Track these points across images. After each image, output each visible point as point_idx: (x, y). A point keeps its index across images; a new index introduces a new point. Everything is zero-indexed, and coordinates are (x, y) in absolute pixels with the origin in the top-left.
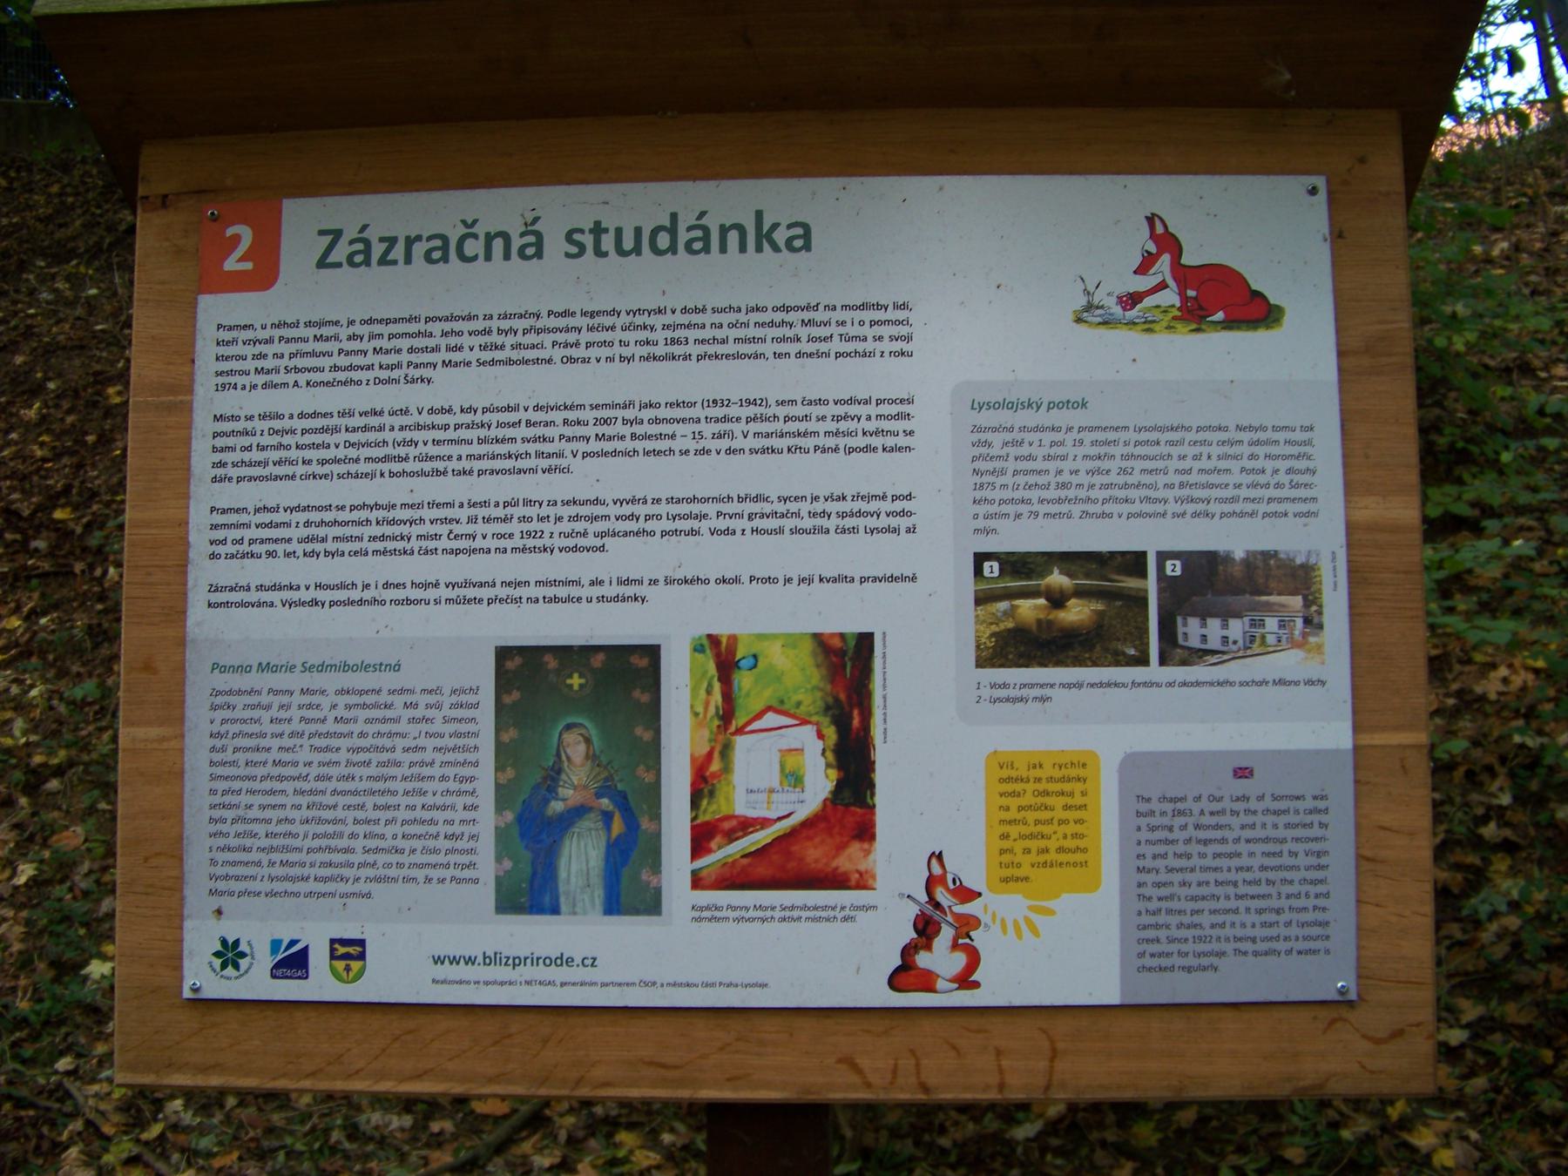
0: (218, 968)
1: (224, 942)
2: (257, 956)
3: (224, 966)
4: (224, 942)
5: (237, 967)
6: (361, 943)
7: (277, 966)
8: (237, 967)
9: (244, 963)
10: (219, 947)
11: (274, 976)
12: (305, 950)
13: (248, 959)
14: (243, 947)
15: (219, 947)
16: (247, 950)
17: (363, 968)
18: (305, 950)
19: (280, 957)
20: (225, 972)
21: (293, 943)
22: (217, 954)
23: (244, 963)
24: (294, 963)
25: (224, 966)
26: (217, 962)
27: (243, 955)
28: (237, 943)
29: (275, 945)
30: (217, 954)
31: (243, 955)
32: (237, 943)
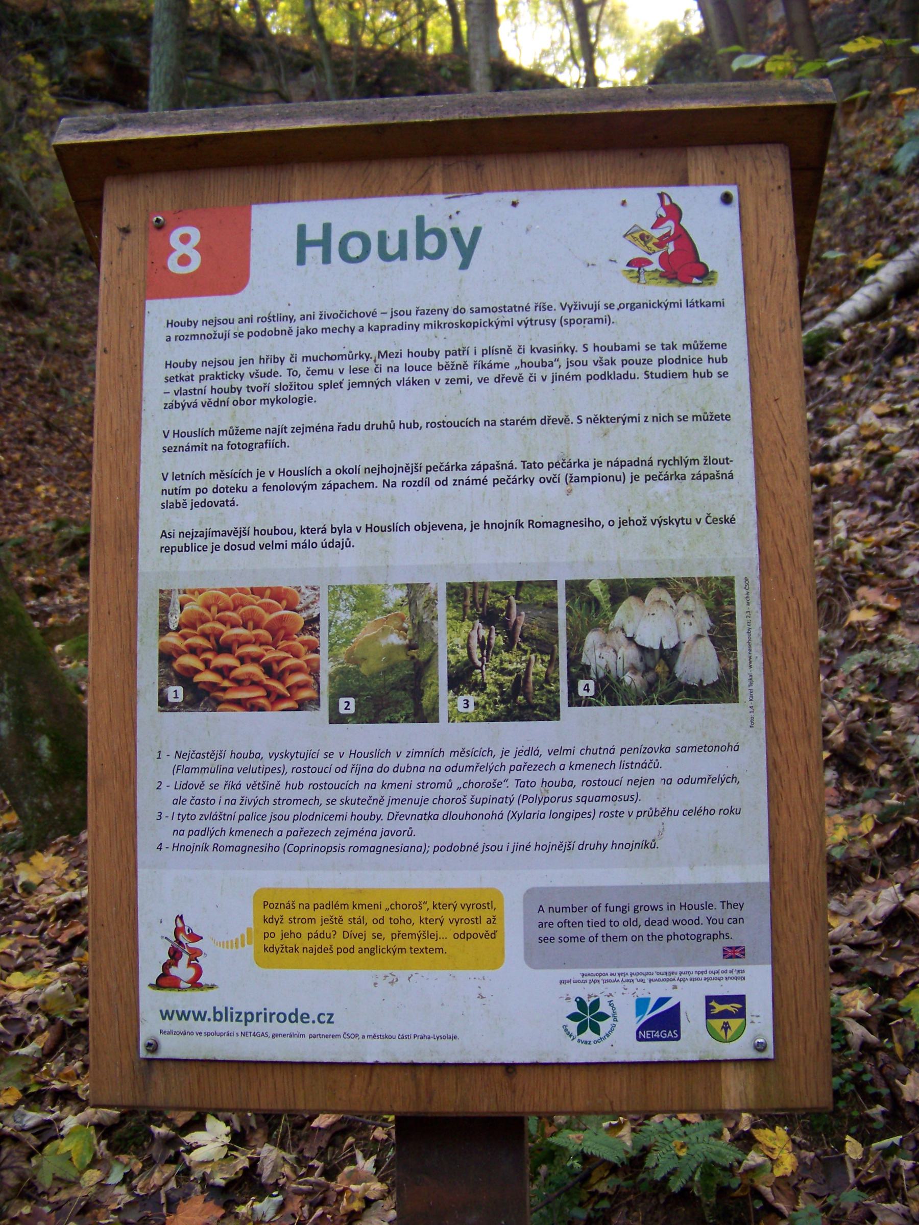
0: (574, 1031)
1: (581, 1003)
3: (581, 1030)
4: (581, 1003)
5: (596, 1030)
6: (741, 999)
7: (642, 1028)
8: (596, 1030)
9: (604, 1026)
10: (574, 1008)
11: (640, 1039)
12: (678, 1005)
13: (610, 1021)
14: (604, 1008)
15: (574, 1008)
16: (608, 1011)
18: (678, 1005)
19: (647, 1017)
20: (583, 1037)
21: (662, 1001)
23: (604, 1026)
25: (581, 1030)
26: (573, 1026)
28: (596, 1004)
29: (641, 1004)
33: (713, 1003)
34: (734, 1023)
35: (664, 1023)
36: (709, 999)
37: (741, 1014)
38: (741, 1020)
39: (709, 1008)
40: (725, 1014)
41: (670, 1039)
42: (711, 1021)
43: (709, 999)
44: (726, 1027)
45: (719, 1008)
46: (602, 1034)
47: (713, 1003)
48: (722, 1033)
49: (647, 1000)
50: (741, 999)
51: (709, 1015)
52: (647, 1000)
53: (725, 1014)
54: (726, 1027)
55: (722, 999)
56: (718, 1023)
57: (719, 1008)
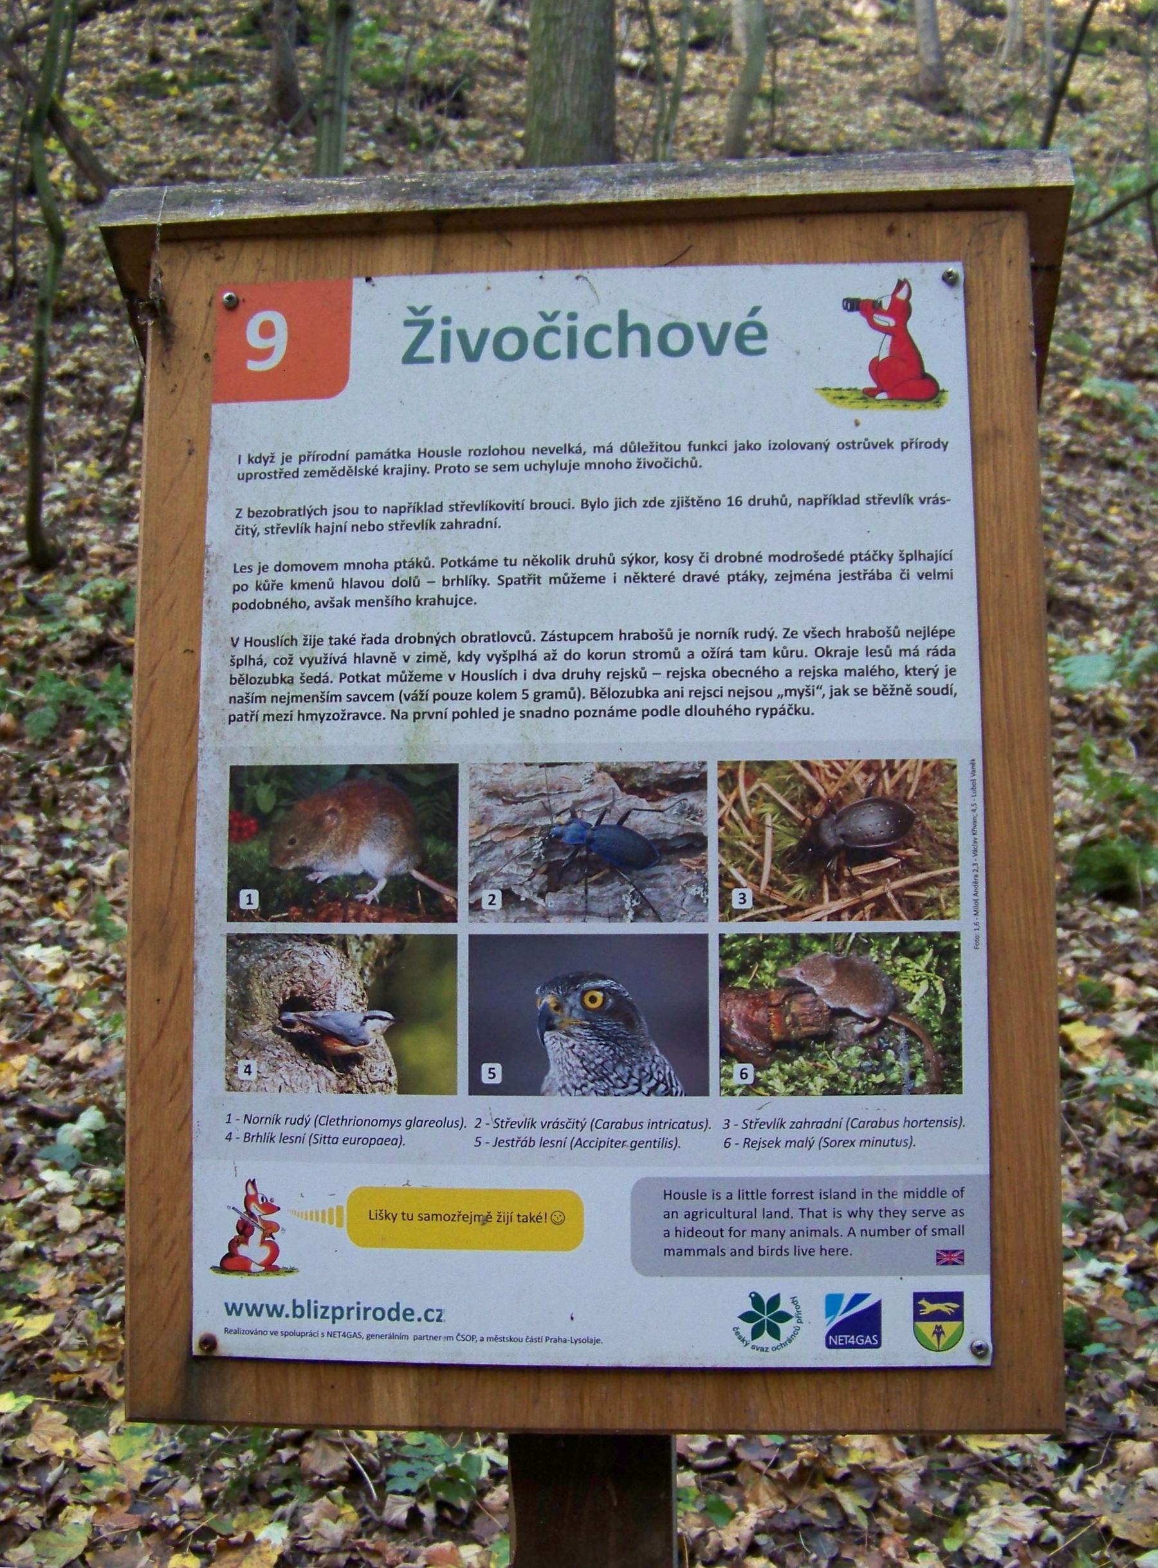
0: (748, 1335)
1: (756, 1300)
2: (804, 1317)
3: (756, 1333)
4: (756, 1300)
5: (775, 1333)
7: (834, 1332)
8: (775, 1333)
9: (785, 1328)
13: (792, 1322)
14: (785, 1306)
17: (961, 1330)
19: (839, 1318)
20: (758, 1342)
21: (858, 1298)
22: (746, 1317)
23: (785, 1328)
24: (863, 1324)
25: (756, 1333)
26: (747, 1328)
27: (784, 1317)
28: (775, 1301)
29: (832, 1302)
30: (746, 1317)
31: (784, 1317)
32: (775, 1301)
33: (923, 1302)
34: (949, 1327)
35: (863, 1324)
36: (917, 1296)
37: (958, 1315)
38: (958, 1324)
39: (917, 1308)
40: (938, 1316)
41: (868, 1346)
42: (920, 1324)
43: (917, 1296)
44: (939, 1332)
45: (929, 1308)
46: (783, 1339)
47: (923, 1302)
48: (934, 1339)
49: (841, 1296)
50: (957, 1297)
51: (918, 1317)
52: (841, 1296)
53: (938, 1316)
54: (939, 1332)
55: (933, 1297)
56: (928, 1328)
57: (929, 1308)
